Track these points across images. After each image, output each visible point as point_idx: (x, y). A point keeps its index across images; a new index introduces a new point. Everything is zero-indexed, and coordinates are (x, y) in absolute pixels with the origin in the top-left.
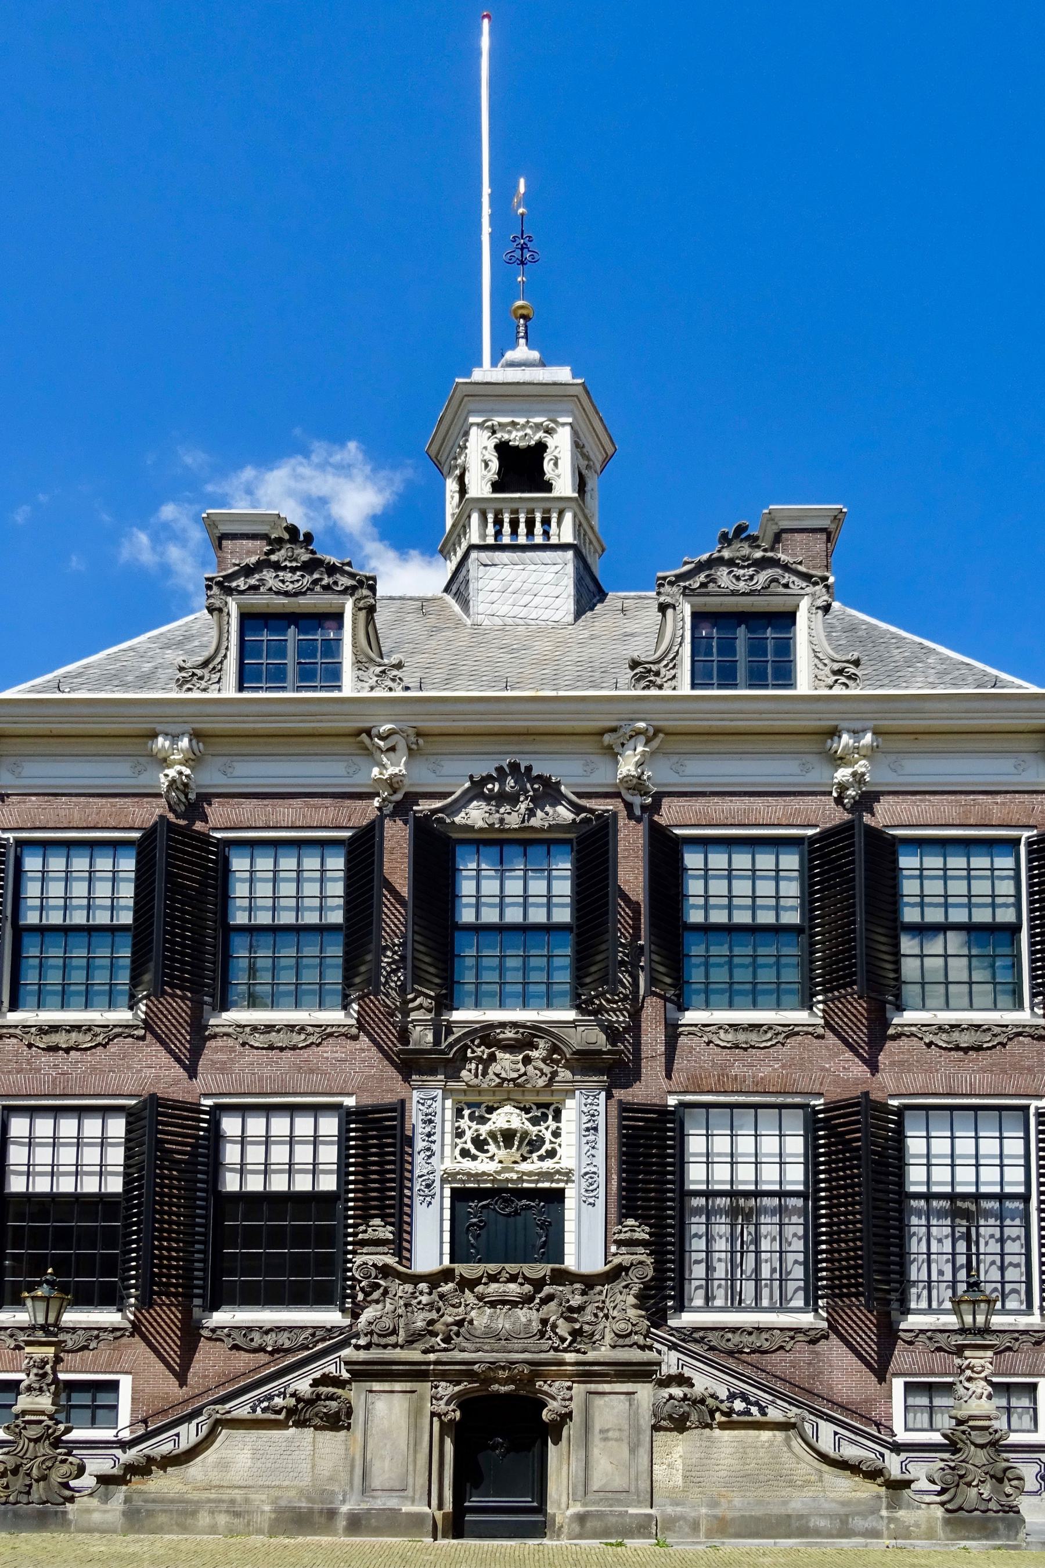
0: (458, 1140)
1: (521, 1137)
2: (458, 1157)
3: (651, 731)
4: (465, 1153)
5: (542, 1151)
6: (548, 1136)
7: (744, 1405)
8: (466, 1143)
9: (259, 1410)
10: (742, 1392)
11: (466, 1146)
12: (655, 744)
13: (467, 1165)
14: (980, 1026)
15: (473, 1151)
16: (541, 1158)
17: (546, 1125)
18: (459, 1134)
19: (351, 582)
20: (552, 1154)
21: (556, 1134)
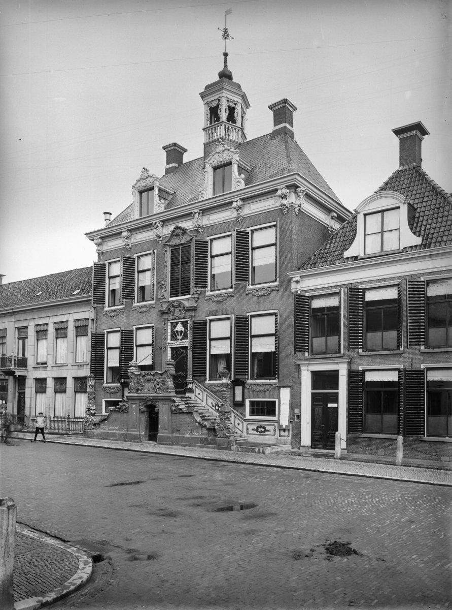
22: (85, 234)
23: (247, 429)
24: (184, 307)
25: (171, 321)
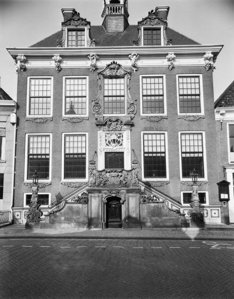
0: (106, 142)
1: (116, 141)
2: (106, 145)
3: (137, 54)
4: (107, 145)
5: (120, 144)
6: (121, 141)
7: (156, 198)
8: (107, 142)
9: (73, 200)
10: (155, 196)
11: (107, 143)
12: (137, 57)
13: (107, 147)
14: (194, 116)
15: (108, 144)
16: (120, 145)
17: (120, 138)
18: (106, 140)
19: (86, 23)
20: (122, 144)
21: (122, 140)
22: (7, 49)
23: (207, 213)
24: (122, 122)
25: (106, 132)
